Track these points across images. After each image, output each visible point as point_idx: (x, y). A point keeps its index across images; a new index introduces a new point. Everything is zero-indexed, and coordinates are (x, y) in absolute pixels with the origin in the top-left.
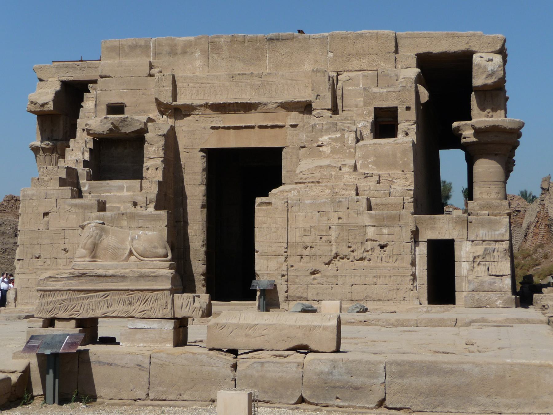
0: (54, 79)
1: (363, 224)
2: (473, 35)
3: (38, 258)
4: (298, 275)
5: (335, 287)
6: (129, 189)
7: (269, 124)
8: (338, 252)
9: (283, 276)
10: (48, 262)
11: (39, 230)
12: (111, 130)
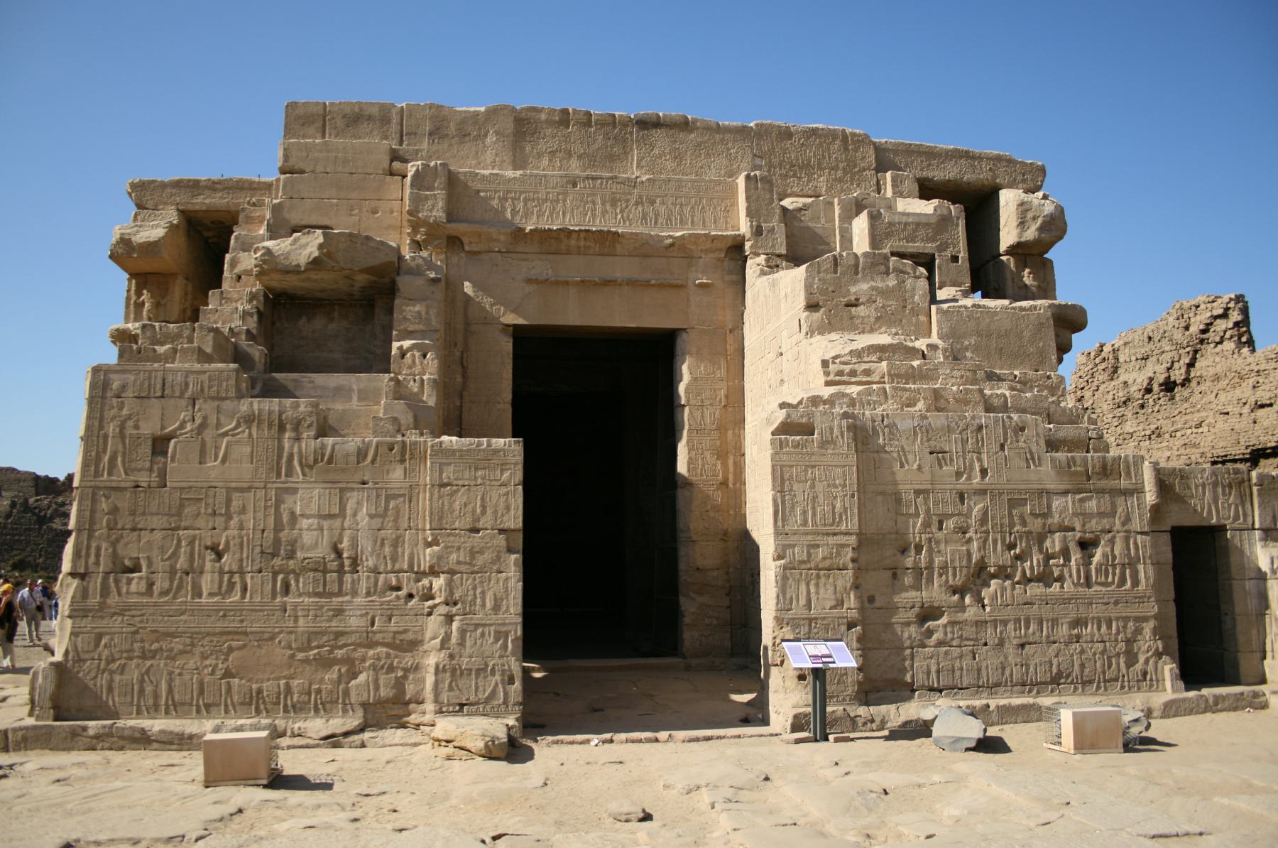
1: (1039, 487)
6: (364, 395)
9: (851, 625)
10: (161, 583)
11: (138, 486)
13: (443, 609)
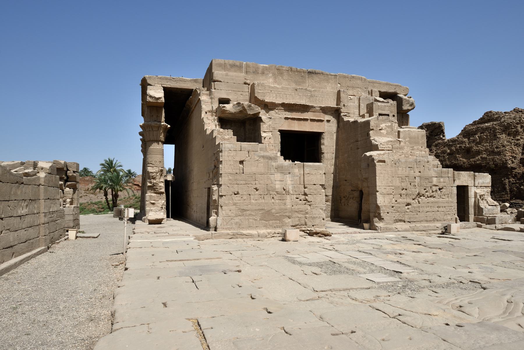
0: (158, 85)
2: (397, 86)
3: (235, 194)
4: (400, 206)
5: (418, 213)
7: (316, 118)
8: (420, 193)
10: (245, 197)
11: (236, 173)
12: (241, 111)
13: (309, 203)
